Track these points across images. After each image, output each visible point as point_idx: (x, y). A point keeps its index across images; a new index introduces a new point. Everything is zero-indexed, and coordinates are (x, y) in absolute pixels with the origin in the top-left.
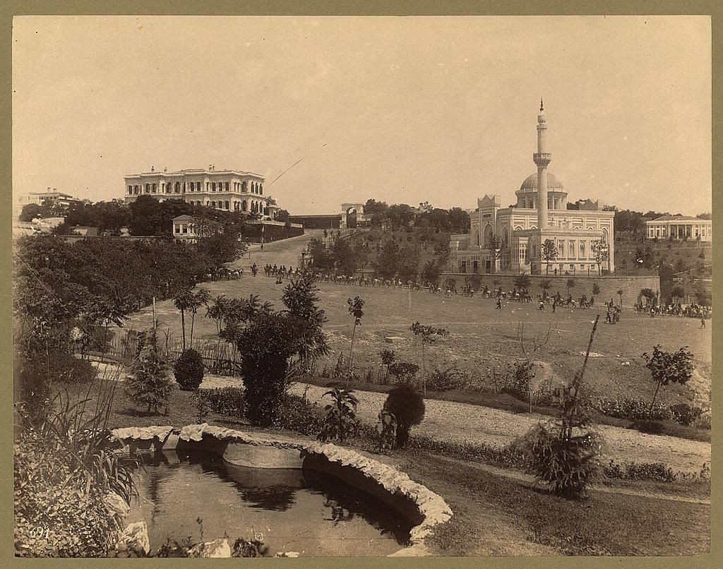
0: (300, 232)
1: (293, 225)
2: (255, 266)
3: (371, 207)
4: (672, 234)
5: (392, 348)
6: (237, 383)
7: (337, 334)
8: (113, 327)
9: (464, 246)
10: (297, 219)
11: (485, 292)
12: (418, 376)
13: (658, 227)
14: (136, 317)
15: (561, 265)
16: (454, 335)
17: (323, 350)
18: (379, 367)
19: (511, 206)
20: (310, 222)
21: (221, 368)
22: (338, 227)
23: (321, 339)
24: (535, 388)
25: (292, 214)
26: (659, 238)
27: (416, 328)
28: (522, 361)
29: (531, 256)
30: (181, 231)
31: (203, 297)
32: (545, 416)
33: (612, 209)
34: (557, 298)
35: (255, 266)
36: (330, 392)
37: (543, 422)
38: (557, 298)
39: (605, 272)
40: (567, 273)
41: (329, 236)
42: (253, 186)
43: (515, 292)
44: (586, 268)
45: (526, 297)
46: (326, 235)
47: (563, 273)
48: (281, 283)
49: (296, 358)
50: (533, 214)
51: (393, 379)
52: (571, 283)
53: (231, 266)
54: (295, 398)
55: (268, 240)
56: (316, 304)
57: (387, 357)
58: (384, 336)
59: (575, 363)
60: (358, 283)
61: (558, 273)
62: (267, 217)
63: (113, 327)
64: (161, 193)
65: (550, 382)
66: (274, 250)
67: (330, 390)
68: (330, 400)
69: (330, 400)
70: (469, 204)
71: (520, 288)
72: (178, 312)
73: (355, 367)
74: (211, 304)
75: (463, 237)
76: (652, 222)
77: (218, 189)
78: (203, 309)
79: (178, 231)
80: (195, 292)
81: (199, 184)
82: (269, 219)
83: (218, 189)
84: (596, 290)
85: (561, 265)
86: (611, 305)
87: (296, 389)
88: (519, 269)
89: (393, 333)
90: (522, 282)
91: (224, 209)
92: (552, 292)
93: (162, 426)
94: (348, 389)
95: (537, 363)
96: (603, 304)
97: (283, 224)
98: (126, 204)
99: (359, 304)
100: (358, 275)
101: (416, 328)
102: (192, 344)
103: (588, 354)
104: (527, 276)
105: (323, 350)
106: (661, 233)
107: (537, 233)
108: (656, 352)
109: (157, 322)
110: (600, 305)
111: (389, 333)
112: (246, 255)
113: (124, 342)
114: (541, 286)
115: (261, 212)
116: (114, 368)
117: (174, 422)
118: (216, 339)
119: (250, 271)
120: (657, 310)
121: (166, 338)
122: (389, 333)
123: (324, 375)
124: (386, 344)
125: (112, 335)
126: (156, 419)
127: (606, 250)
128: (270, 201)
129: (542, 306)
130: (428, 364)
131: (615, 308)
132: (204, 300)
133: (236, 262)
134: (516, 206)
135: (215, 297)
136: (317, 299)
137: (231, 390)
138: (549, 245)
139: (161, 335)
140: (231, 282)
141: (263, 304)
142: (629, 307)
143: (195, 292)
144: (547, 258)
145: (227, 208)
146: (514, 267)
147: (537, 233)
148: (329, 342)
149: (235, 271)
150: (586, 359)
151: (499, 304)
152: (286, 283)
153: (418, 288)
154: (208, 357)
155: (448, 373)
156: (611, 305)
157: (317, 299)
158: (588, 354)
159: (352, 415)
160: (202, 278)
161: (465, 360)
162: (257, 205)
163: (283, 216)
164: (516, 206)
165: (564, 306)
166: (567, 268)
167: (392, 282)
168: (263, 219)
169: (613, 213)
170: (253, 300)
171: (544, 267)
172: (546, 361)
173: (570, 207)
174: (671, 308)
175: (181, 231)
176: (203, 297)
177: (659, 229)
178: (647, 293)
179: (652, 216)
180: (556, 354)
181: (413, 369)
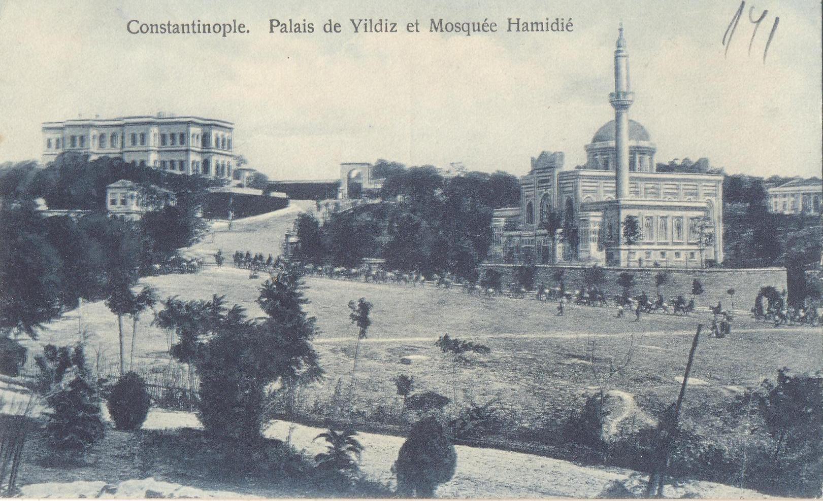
0: (282, 204)
1: (274, 194)
2: (220, 253)
3: (381, 169)
4: (804, 207)
5: (409, 371)
7: (334, 351)
8: (24, 339)
9: (511, 225)
10: (279, 187)
11: (541, 292)
12: (447, 410)
13: (784, 196)
14: (55, 326)
15: (648, 253)
16: (497, 354)
17: (316, 373)
18: (394, 400)
19: (578, 167)
20: (300, 191)
21: (172, 401)
22: (335, 197)
23: (312, 358)
24: (611, 429)
25: (273, 177)
26: (786, 213)
27: (446, 343)
28: (593, 390)
29: (608, 242)
30: (119, 202)
31: (147, 298)
32: (625, 470)
33: (719, 172)
34: (643, 301)
35: (220, 253)
36: (322, 435)
37: (621, 478)
38: (643, 301)
39: (711, 263)
40: (656, 265)
41: (324, 210)
42: (217, 139)
43: (583, 292)
44: (682, 258)
45: (600, 299)
46: (319, 207)
47: (651, 264)
48: (256, 277)
49: (276, 385)
50: (610, 178)
51: (413, 417)
52: (661, 279)
53: (187, 253)
54: (276, 443)
55: (239, 215)
56: (304, 308)
57: (404, 384)
58: (401, 355)
59: (665, 392)
60: (363, 278)
61: (644, 264)
62: (239, 182)
63: (24, 339)
64: (94, 150)
65: (632, 420)
66: (249, 229)
67: (325, 431)
68: (323, 447)
69: (323, 447)
70: (519, 169)
71: (590, 284)
72: (114, 317)
73: (359, 400)
74: (160, 308)
75: (509, 211)
76: (776, 189)
77: (169, 141)
78: (148, 314)
79: (113, 202)
80: (137, 290)
81: (182, 136)
82: (240, 186)
83: (169, 141)
84: (697, 288)
85: (648, 253)
86: (717, 310)
87: (276, 430)
88: (589, 259)
89: (413, 350)
90: (595, 275)
91: (178, 172)
92: (639, 290)
93: (91, 480)
94: (350, 429)
95: (612, 393)
96: (707, 309)
97: (259, 192)
98: (51, 168)
99: (365, 307)
100: (365, 267)
101: (446, 343)
102: (133, 364)
103: (685, 381)
104: (601, 269)
105: (316, 373)
106: (789, 205)
107: (614, 206)
108: (782, 377)
109: (84, 334)
110: (702, 308)
111: (407, 350)
112: (208, 238)
113: (39, 361)
114: (619, 282)
115: (229, 175)
116: (26, 398)
117: (108, 476)
118: (166, 357)
119: (213, 260)
120: (782, 317)
121: (96, 356)
122: (407, 350)
123: (317, 410)
124: (404, 367)
125: (23, 351)
126: (84, 472)
127: (711, 230)
128: (241, 160)
129: (621, 312)
130: (460, 394)
131: (724, 314)
132: (151, 303)
133: (195, 247)
134: (585, 167)
135: (165, 298)
136: (305, 301)
137: (187, 431)
138: (631, 224)
139: (89, 353)
140: (187, 276)
141: (231, 307)
142: (742, 313)
143: (137, 290)
144: (630, 243)
145: (182, 168)
146: (583, 255)
147: (614, 206)
148: (322, 362)
149: (192, 260)
150: (683, 389)
151: (560, 308)
152: (265, 277)
153: (448, 285)
154: (155, 386)
155: (489, 408)
156: (717, 310)
157: (305, 301)
158: (685, 381)
159: (355, 467)
160: (148, 271)
161: (513, 390)
162: (223, 167)
163: (258, 181)
164: (585, 167)
165: (652, 312)
166: (656, 257)
167: (411, 278)
168: (232, 187)
169: (721, 178)
170: (217, 301)
171: (623, 255)
172: (627, 390)
173: (662, 168)
174: (802, 314)
175: (119, 202)
176: (147, 298)
177: (786, 199)
178: (769, 292)
179: (777, 181)
180: (638, 380)
181: (443, 401)
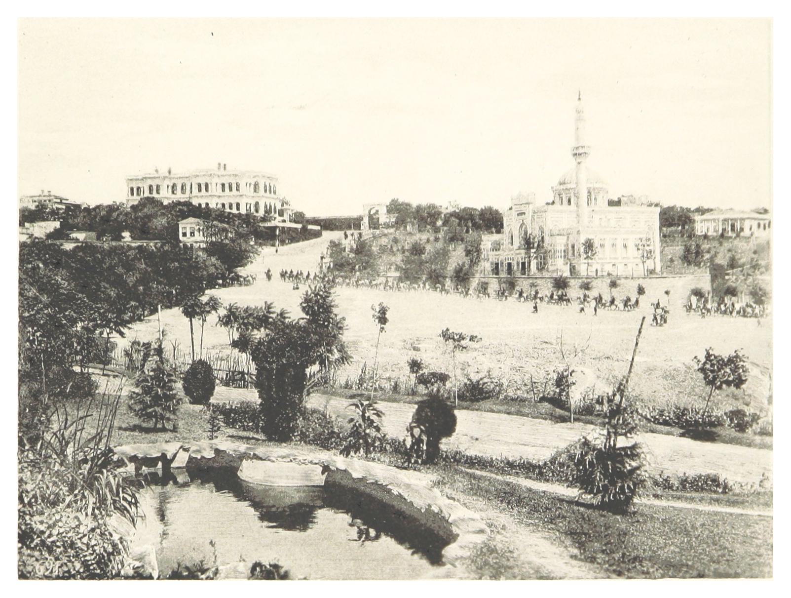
0: (317, 234)
1: (310, 227)
6: (252, 396)
8: (115, 337)
9: (497, 247)
10: (315, 222)
11: (521, 295)
12: (448, 385)
14: (137, 326)
15: (603, 264)
17: (344, 359)
20: (329, 225)
24: (576, 397)
25: (309, 215)
27: (446, 335)
30: (188, 235)
31: (214, 304)
38: (599, 300)
40: (609, 274)
41: (350, 237)
42: (265, 186)
44: (630, 266)
45: (566, 300)
46: (346, 236)
48: (298, 288)
49: (315, 368)
53: (242, 271)
55: (283, 242)
57: (415, 365)
63: (115, 337)
68: (355, 413)
69: (355, 413)
74: (222, 312)
75: (496, 237)
78: (213, 318)
79: (184, 234)
80: (204, 299)
82: (284, 221)
85: (603, 264)
90: (561, 284)
91: (234, 211)
97: (299, 226)
99: (383, 311)
104: (567, 278)
105: (344, 359)
108: (708, 356)
109: (163, 332)
113: (127, 354)
114: (581, 287)
115: (275, 212)
120: (709, 311)
123: (347, 386)
130: (458, 372)
131: (663, 309)
133: (249, 266)
139: (167, 346)
141: (279, 311)
143: (204, 299)
146: (551, 268)
151: (535, 308)
152: (304, 288)
156: (658, 305)
159: (378, 429)
160: (212, 285)
162: (270, 206)
163: (299, 217)
167: (419, 286)
169: (658, 210)
170: (269, 307)
175: (188, 235)
176: (214, 304)
178: (698, 293)
179: (701, 211)
181: (443, 378)
